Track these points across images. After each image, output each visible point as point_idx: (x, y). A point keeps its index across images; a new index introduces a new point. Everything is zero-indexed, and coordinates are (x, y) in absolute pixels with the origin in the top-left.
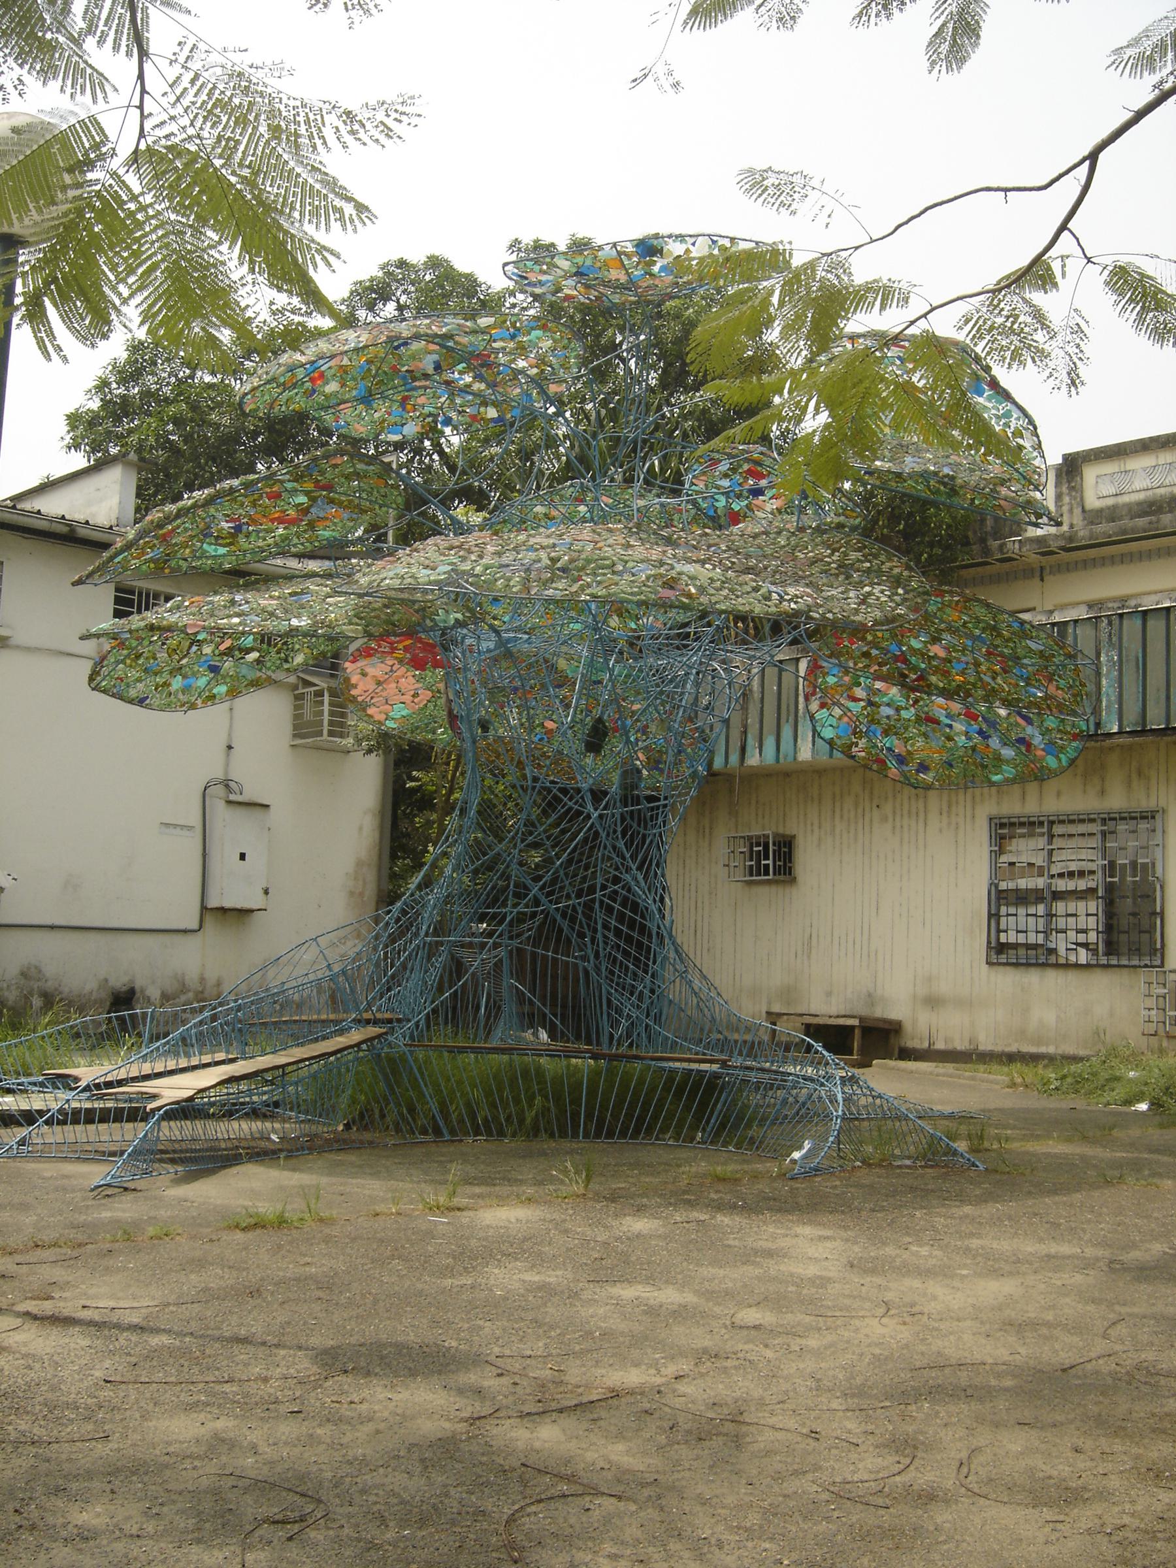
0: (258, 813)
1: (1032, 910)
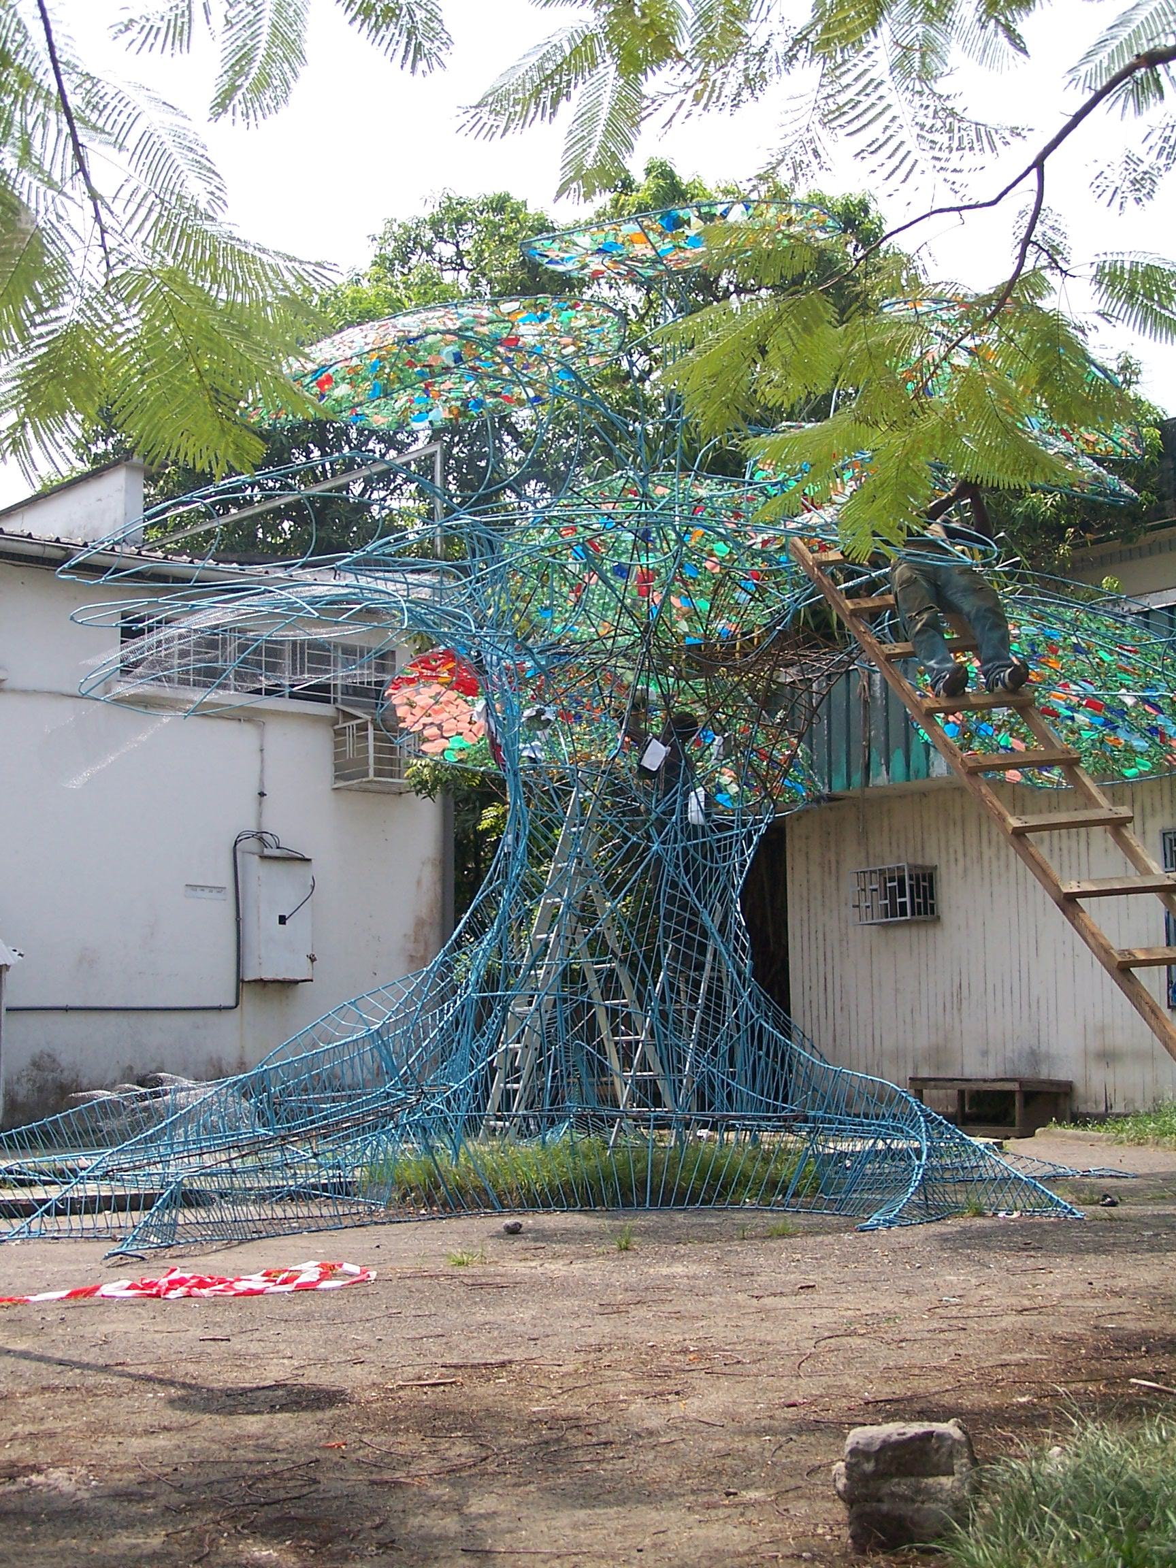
0: (298, 867)
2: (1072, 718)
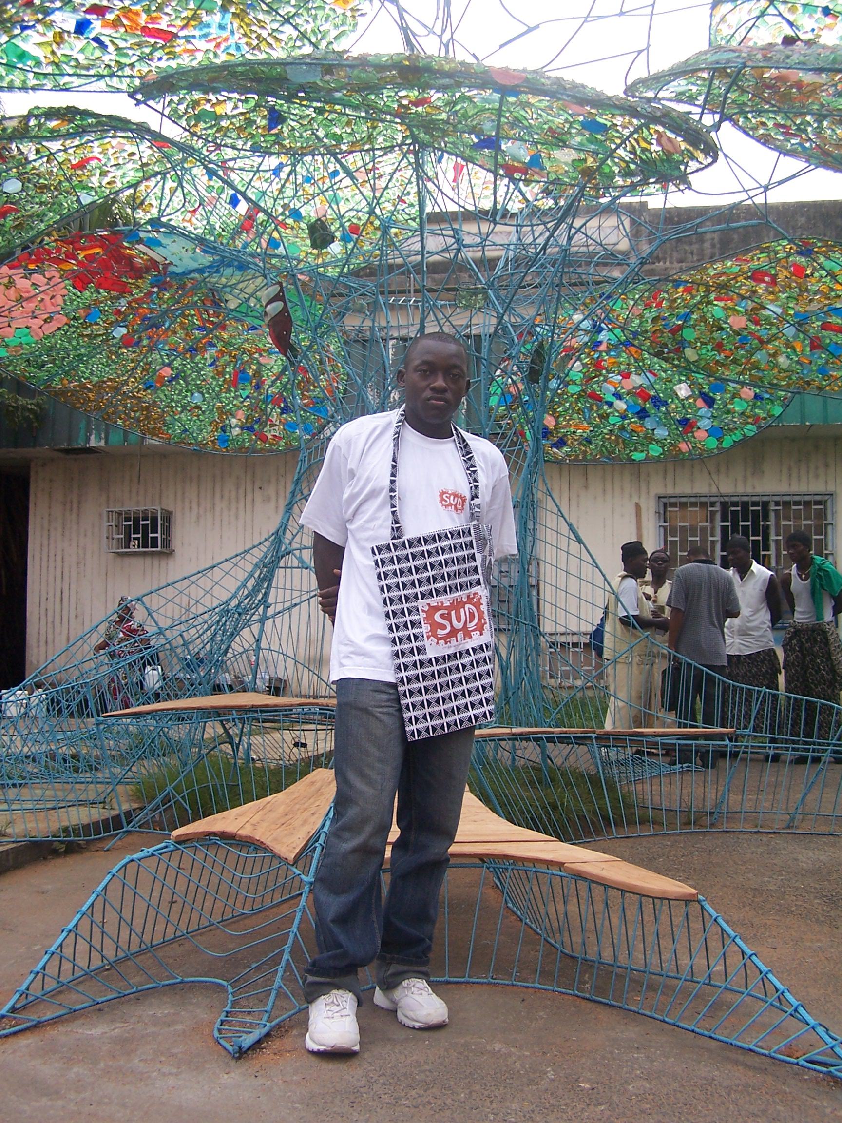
2: (611, 404)
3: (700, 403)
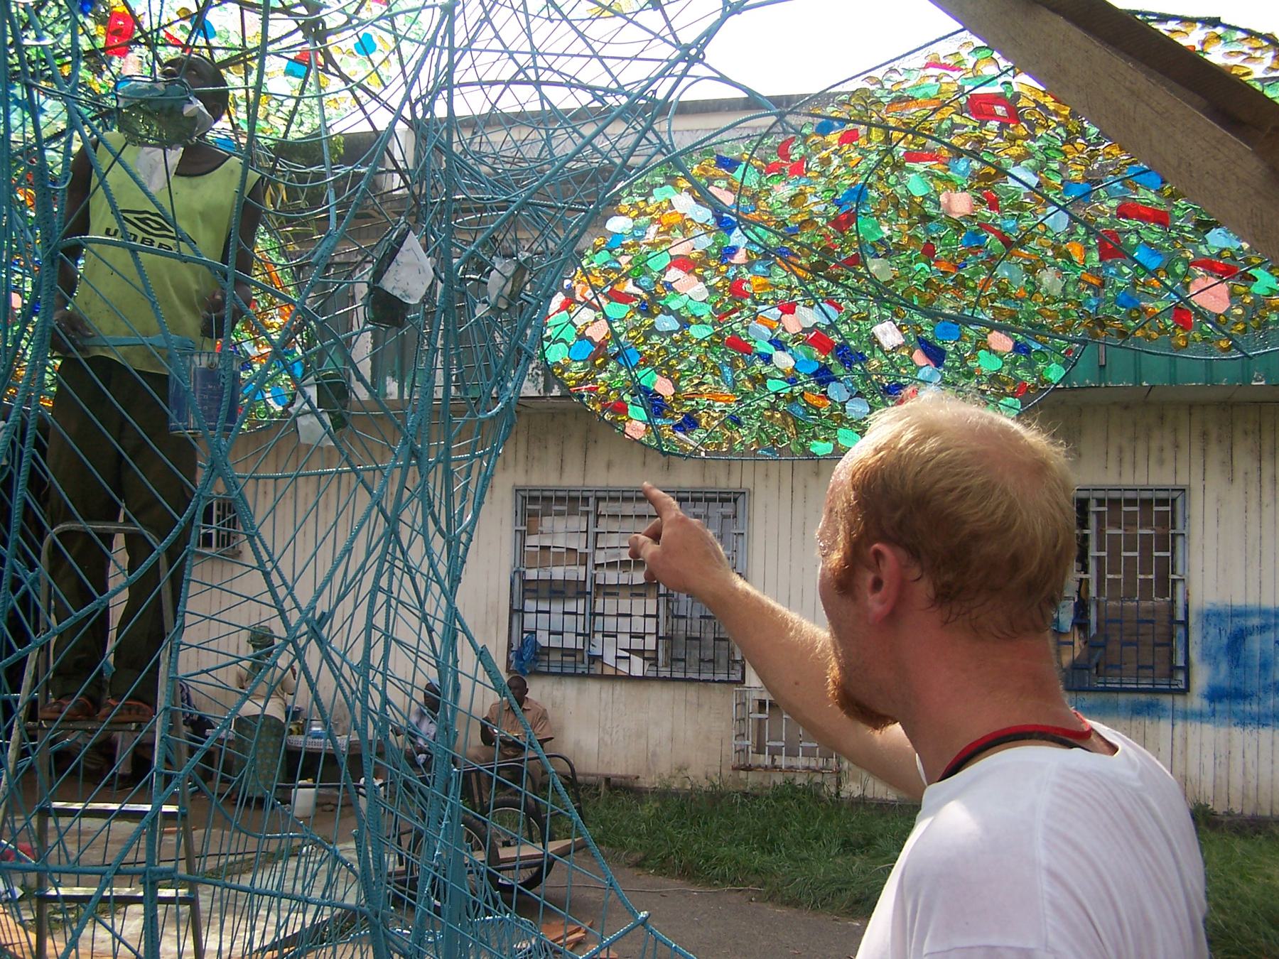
1: (571, 606)
2: (768, 359)
3: (919, 357)
